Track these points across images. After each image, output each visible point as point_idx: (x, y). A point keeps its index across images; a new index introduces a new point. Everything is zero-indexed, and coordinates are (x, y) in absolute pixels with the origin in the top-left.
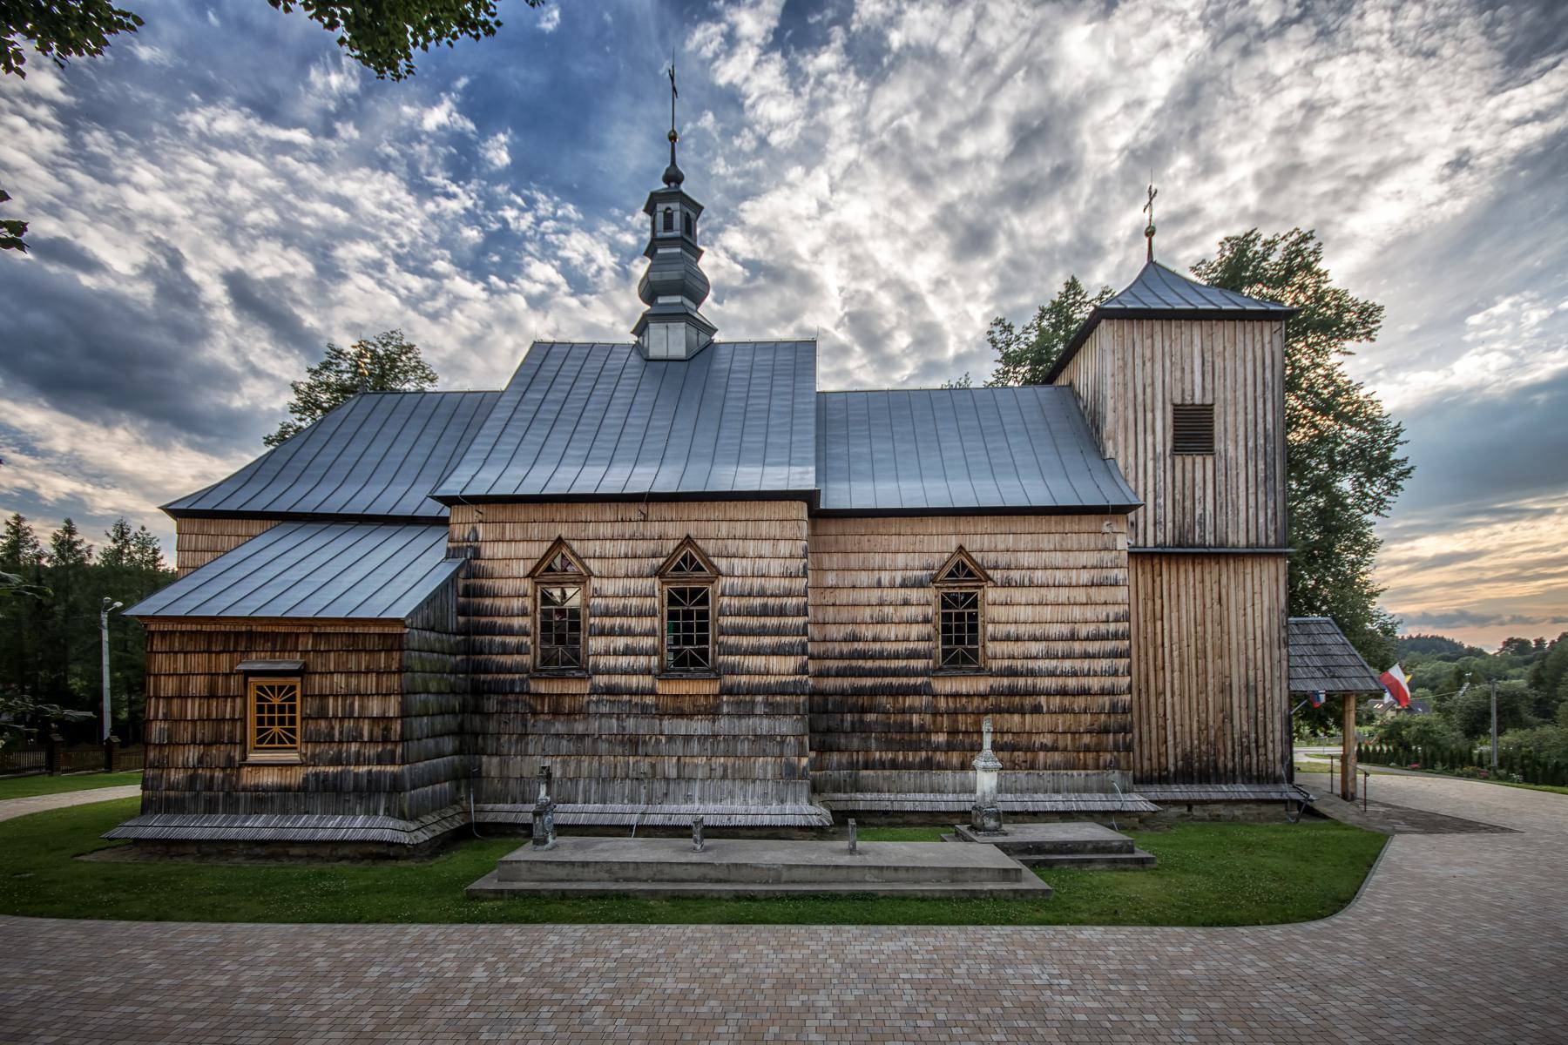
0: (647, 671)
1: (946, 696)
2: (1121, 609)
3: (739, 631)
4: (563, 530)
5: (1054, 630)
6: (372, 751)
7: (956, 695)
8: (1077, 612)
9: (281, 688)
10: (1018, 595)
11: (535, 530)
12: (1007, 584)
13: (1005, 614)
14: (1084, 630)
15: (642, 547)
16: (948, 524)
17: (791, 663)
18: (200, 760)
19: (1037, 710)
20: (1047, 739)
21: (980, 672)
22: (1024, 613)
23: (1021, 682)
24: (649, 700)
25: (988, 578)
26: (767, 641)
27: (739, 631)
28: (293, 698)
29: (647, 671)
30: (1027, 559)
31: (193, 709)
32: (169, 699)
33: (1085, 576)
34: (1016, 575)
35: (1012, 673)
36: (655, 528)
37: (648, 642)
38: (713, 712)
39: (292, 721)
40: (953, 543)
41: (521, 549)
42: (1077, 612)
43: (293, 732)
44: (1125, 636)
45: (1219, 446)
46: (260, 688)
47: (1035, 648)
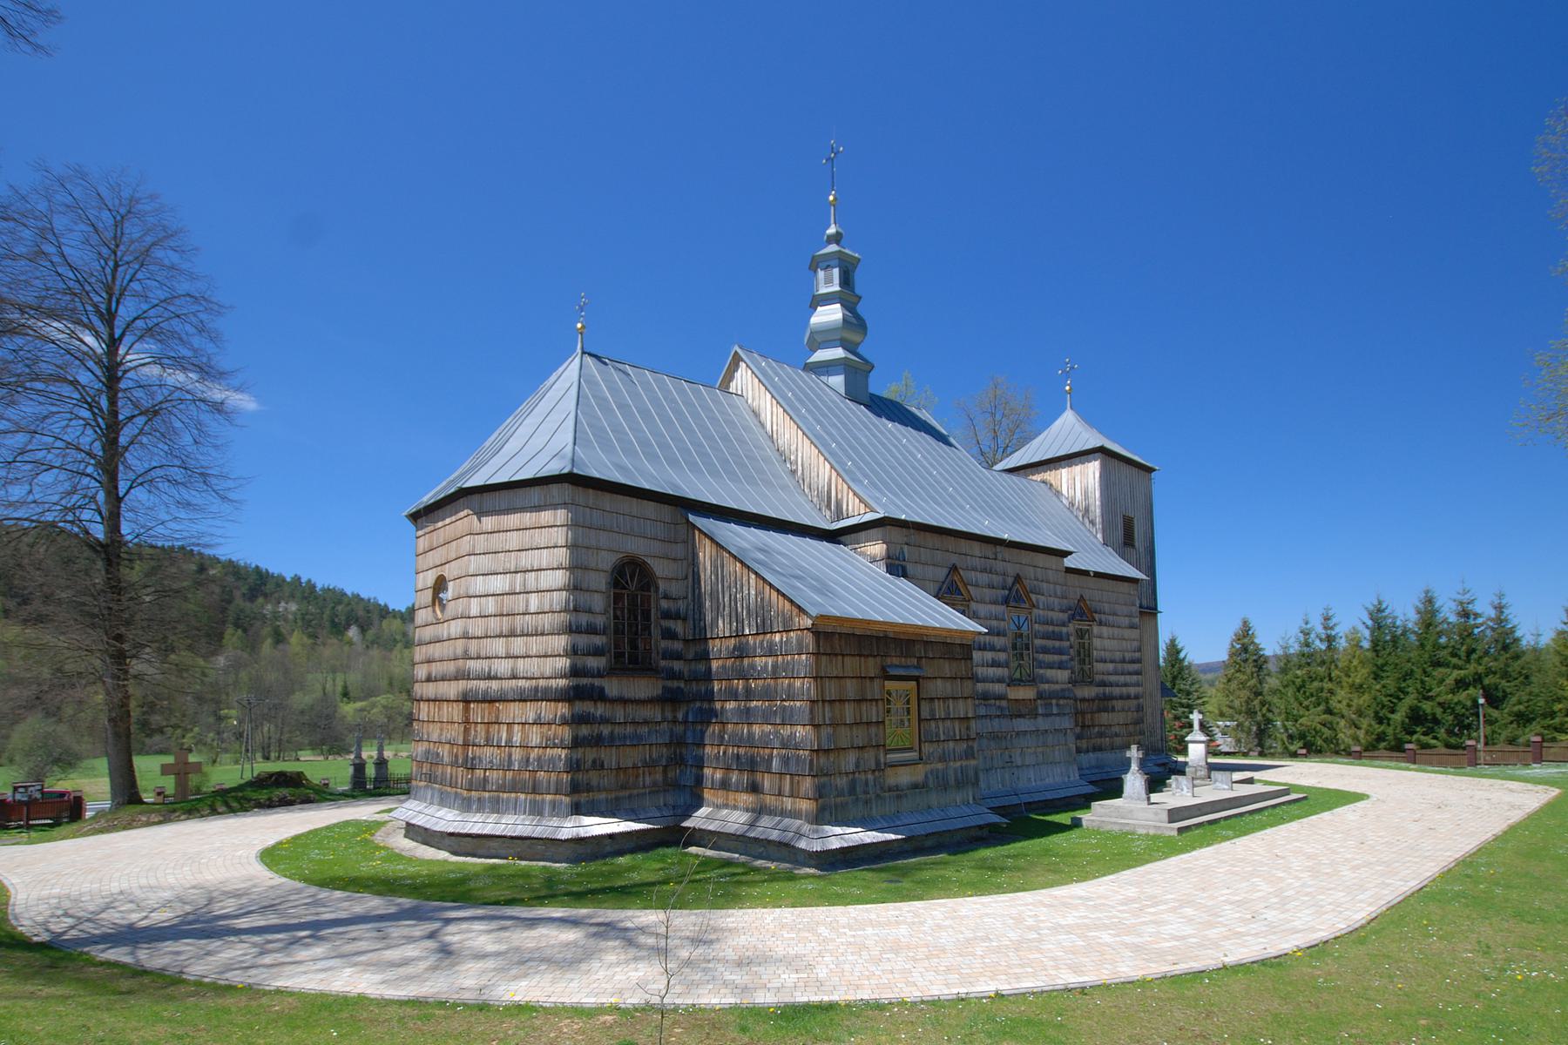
0: (1000, 680)
2: (1135, 644)
3: (1045, 650)
5: (1118, 655)
10: (1105, 630)
12: (1100, 624)
14: (1128, 656)
15: (996, 579)
18: (857, 765)
19: (1113, 710)
22: (1107, 643)
23: (1107, 689)
24: (1004, 703)
26: (1056, 658)
27: (1045, 650)
29: (1000, 680)
30: (1106, 607)
34: (1103, 617)
35: (1103, 684)
36: (999, 566)
37: (1002, 656)
38: (1034, 715)
44: (1139, 661)
47: (1111, 666)
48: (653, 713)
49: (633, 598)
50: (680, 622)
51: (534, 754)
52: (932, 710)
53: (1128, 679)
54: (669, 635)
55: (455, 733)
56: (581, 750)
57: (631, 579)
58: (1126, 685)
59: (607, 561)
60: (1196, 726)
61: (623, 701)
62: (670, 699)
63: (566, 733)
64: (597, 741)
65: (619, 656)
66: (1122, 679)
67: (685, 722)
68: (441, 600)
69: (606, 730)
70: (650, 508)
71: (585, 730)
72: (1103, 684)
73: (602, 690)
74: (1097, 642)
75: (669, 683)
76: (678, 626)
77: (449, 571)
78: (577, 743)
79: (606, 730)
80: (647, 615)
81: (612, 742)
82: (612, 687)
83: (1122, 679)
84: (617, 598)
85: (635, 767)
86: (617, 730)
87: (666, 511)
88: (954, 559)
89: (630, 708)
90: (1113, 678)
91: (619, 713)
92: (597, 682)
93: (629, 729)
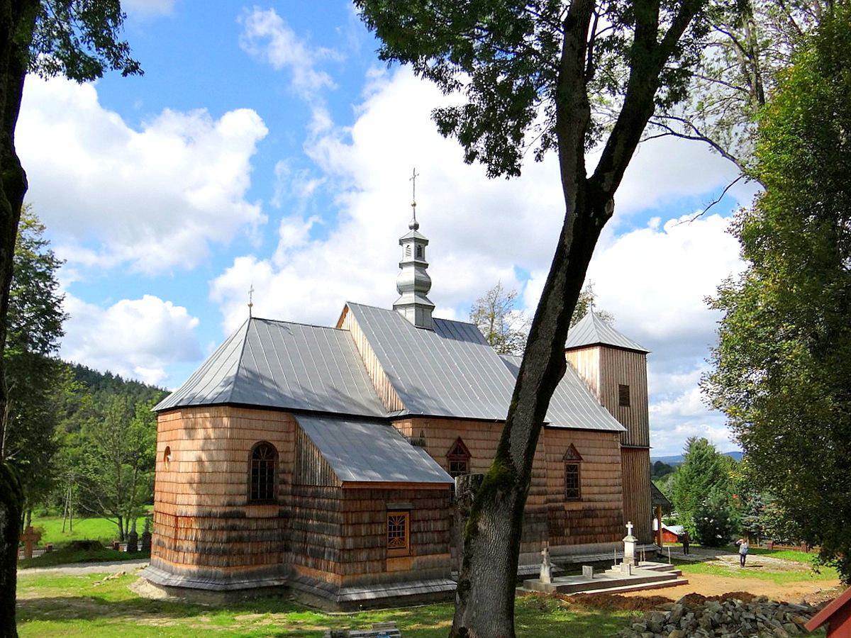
1: (569, 511)
5: (603, 482)
6: (439, 547)
7: (572, 511)
8: (607, 475)
9: (399, 517)
10: (590, 466)
11: (448, 433)
13: (587, 474)
16: (567, 434)
17: (542, 499)
19: (597, 517)
20: (600, 529)
21: (580, 500)
22: (593, 474)
25: (581, 459)
28: (403, 523)
31: (363, 530)
32: (353, 524)
33: (610, 459)
39: (403, 534)
40: (571, 441)
41: (441, 442)
42: (607, 475)
43: (403, 539)
46: (404, 517)
47: (596, 490)
48: (275, 524)
49: (263, 464)
50: (290, 475)
51: (208, 546)
52: (419, 527)
53: (611, 497)
54: (284, 482)
55: (171, 532)
56: (231, 545)
57: (263, 456)
58: (607, 501)
59: (250, 445)
60: (629, 533)
61: (257, 519)
62: (284, 516)
63: (224, 536)
64: (240, 540)
65: (254, 495)
67: (291, 528)
68: (168, 459)
69: (246, 534)
70: (275, 416)
71: (234, 534)
72: (589, 501)
73: (245, 513)
74: (583, 474)
75: (283, 508)
76: (290, 479)
77: (173, 446)
78: (229, 541)
79: (246, 534)
80: (271, 472)
81: (249, 540)
82: (252, 512)
84: (255, 464)
85: (262, 553)
86: (253, 534)
87: (283, 417)
88: (458, 434)
89: (260, 523)
90: (597, 497)
91: (254, 525)
92: (241, 509)
93: (259, 533)
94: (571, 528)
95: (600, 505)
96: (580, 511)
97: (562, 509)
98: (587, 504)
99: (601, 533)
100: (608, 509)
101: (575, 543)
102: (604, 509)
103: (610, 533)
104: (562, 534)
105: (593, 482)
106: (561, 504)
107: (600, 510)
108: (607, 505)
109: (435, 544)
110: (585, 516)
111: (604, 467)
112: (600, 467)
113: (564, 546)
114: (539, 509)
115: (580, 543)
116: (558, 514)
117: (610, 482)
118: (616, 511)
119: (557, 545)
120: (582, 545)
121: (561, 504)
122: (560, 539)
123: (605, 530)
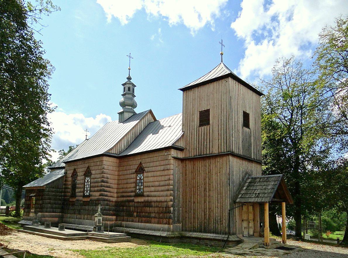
4: (76, 167)
7: (138, 202)
8: (160, 179)
10: (150, 174)
19: (152, 207)
20: (153, 215)
22: (151, 179)
42: (160, 179)
45: (211, 122)
53: (162, 193)
66: (156, 193)
72: (148, 196)
83: (156, 193)
90: (153, 194)
94: (137, 212)
95: (154, 199)
96: (143, 202)
97: (133, 201)
98: (146, 199)
99: (155, 218)
100: (159, 202)
101: (138, 222)
102: (157, 202)
103: (160, 218)
104: (132, 215)
105: (150, 184)
106: (132, 198)
107: (154, 202)
108: (159, 199)
109: (39, 208)
110: (145, 206)
111: (158, 173)
112: (155, 174)
113: (132, 222)
114: (97, 199)
115: (141, 222)
116: (131, 204)
117: (162, 183)
118: (165, 203)
119: (129, 222)
120: (142, 224)
121: (132, 198)
122: (130, 219)
123: (157, 215)
